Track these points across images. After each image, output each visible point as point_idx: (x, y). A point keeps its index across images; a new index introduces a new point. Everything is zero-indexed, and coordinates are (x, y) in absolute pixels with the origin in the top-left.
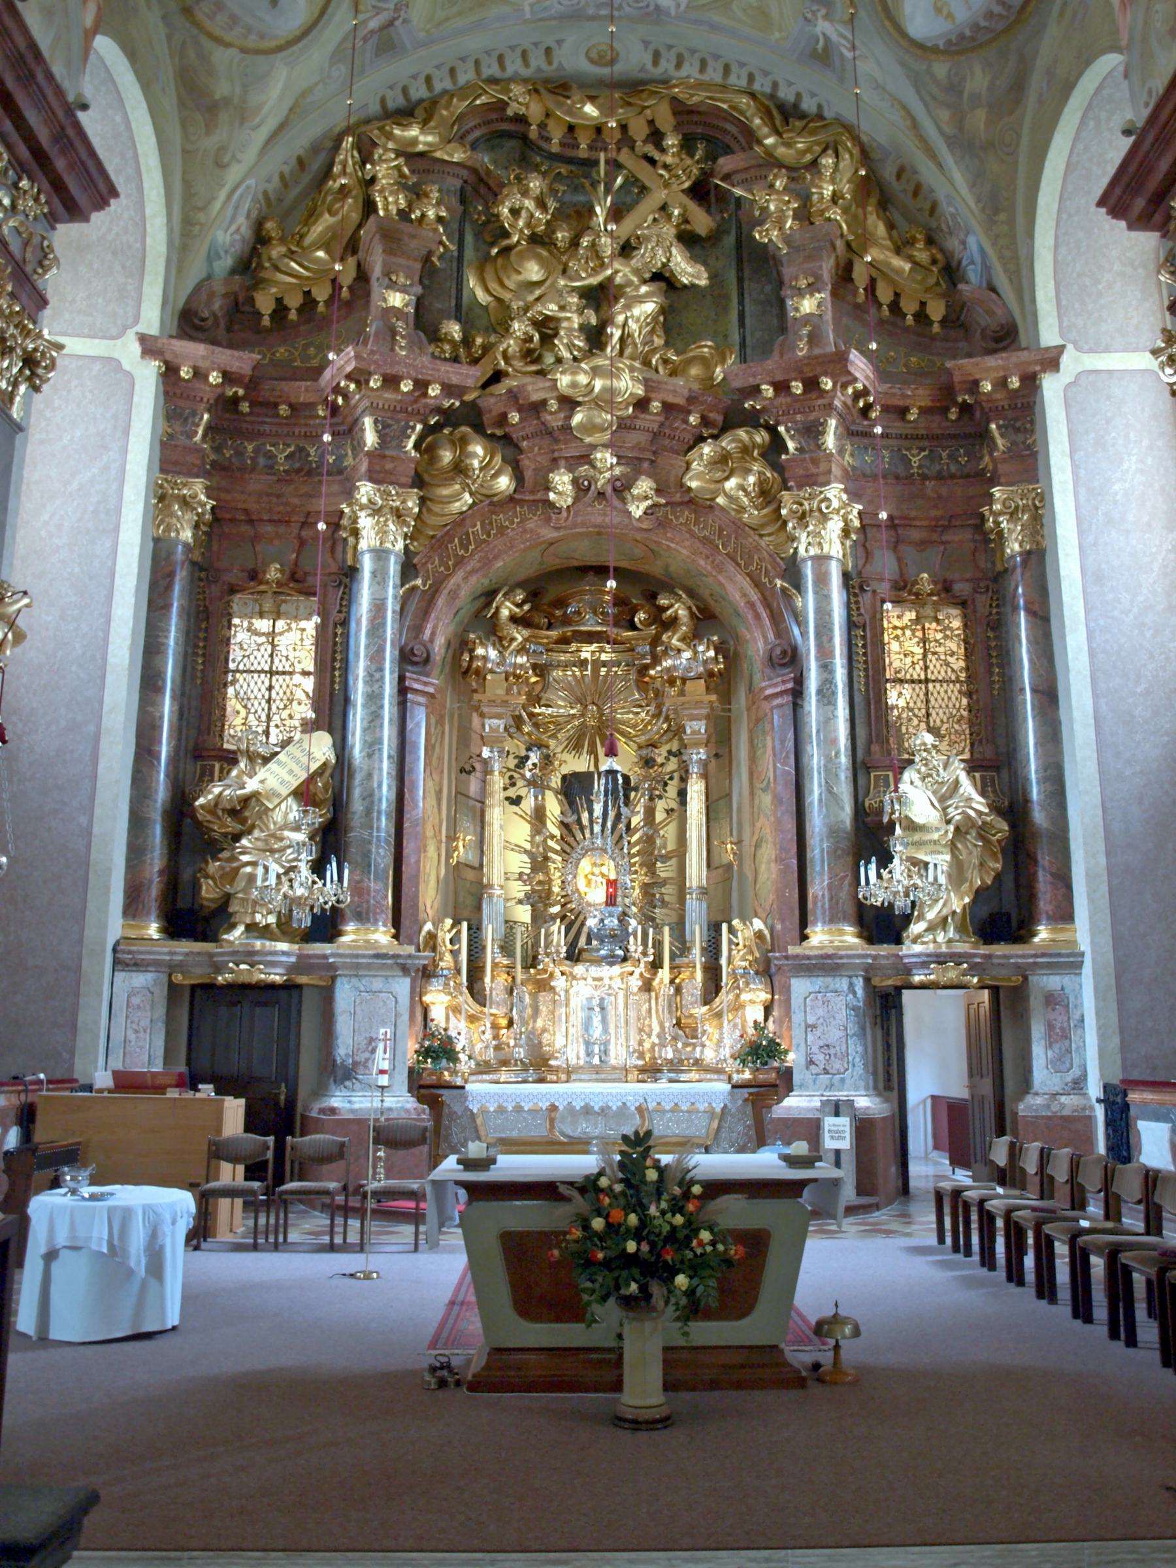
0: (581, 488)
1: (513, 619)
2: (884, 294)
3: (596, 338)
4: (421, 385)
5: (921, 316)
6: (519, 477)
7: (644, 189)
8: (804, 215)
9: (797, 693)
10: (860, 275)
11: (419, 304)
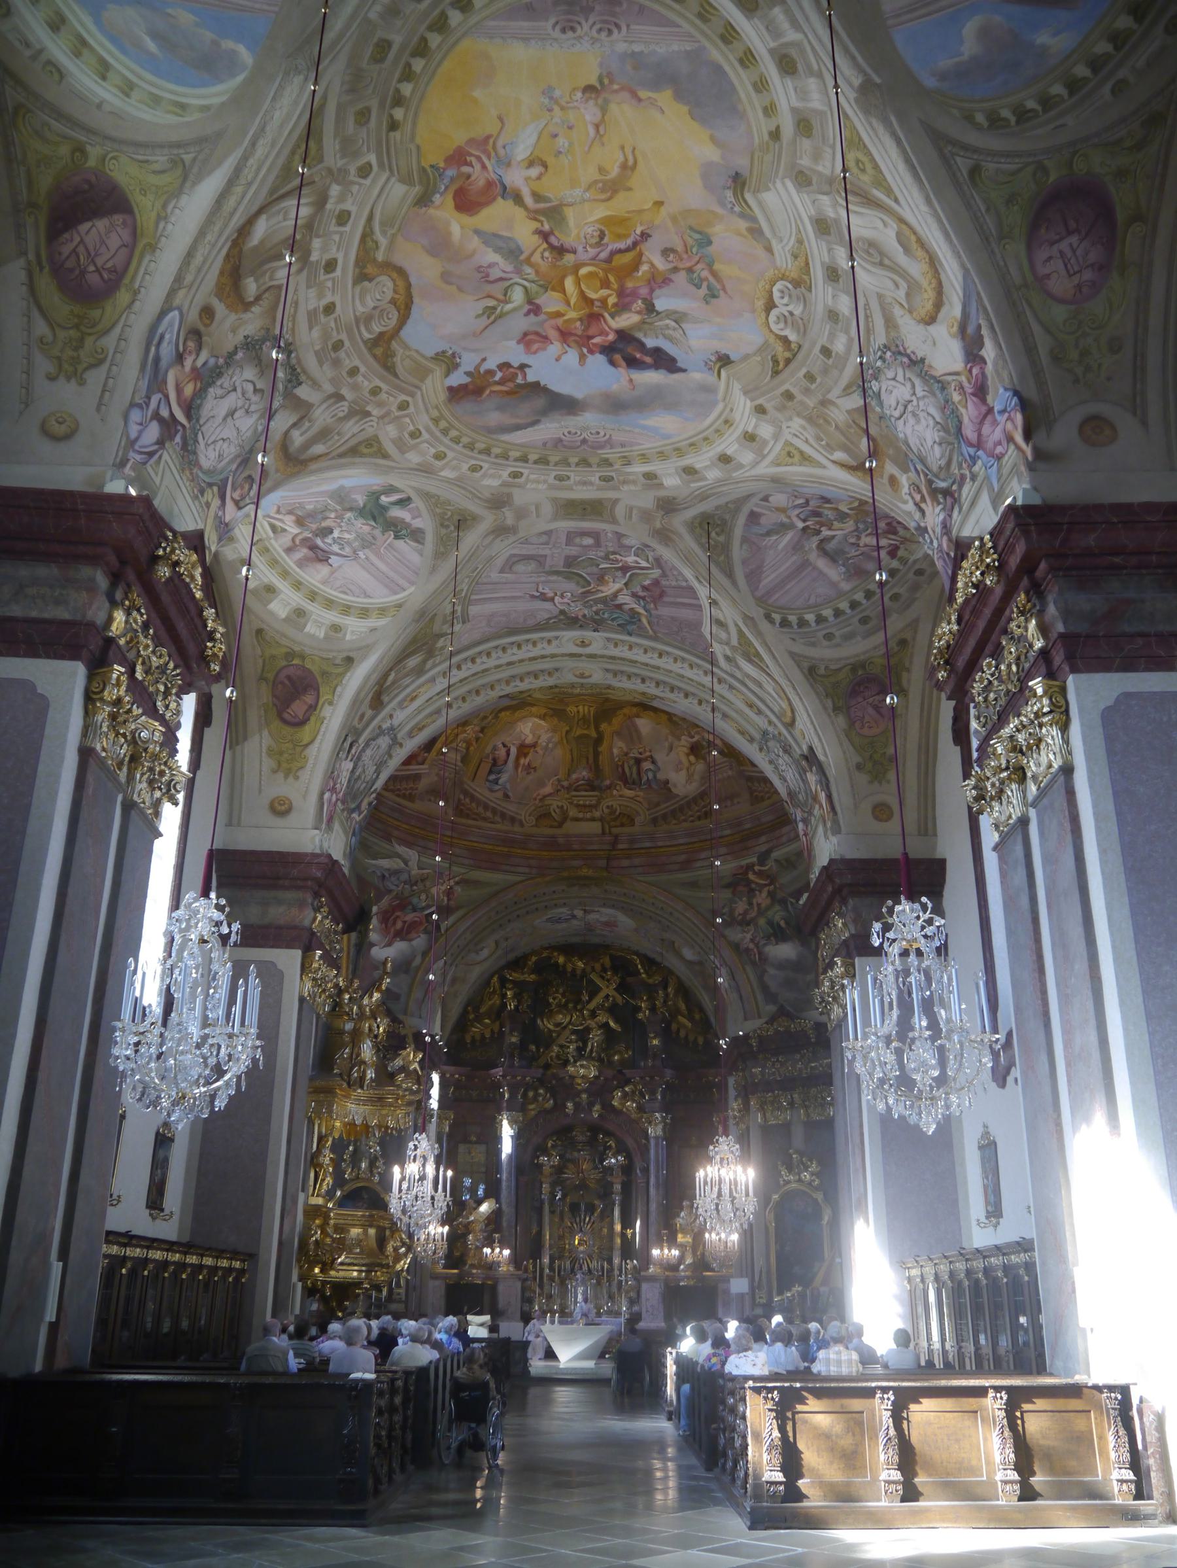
0: (577, 1106)
1: (553, 1146)
2: (682, 1034)
3: (580, 1050)
4: (524, 1077)
5: (696, 1039)
6: (555, 1101)
7: (599, 989)
8: (653, 1009)
9: (648, 1183)
10: (674, 1026)
11: (521, 1041)
